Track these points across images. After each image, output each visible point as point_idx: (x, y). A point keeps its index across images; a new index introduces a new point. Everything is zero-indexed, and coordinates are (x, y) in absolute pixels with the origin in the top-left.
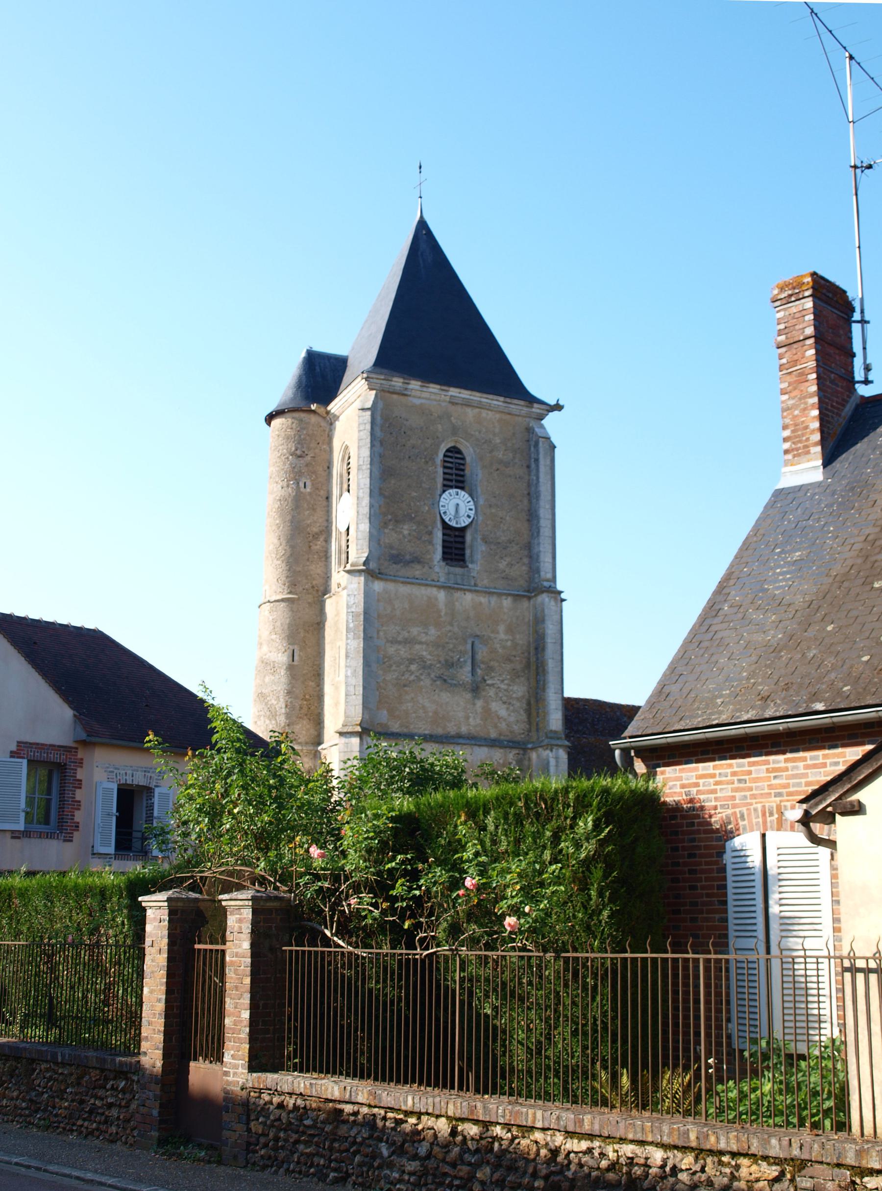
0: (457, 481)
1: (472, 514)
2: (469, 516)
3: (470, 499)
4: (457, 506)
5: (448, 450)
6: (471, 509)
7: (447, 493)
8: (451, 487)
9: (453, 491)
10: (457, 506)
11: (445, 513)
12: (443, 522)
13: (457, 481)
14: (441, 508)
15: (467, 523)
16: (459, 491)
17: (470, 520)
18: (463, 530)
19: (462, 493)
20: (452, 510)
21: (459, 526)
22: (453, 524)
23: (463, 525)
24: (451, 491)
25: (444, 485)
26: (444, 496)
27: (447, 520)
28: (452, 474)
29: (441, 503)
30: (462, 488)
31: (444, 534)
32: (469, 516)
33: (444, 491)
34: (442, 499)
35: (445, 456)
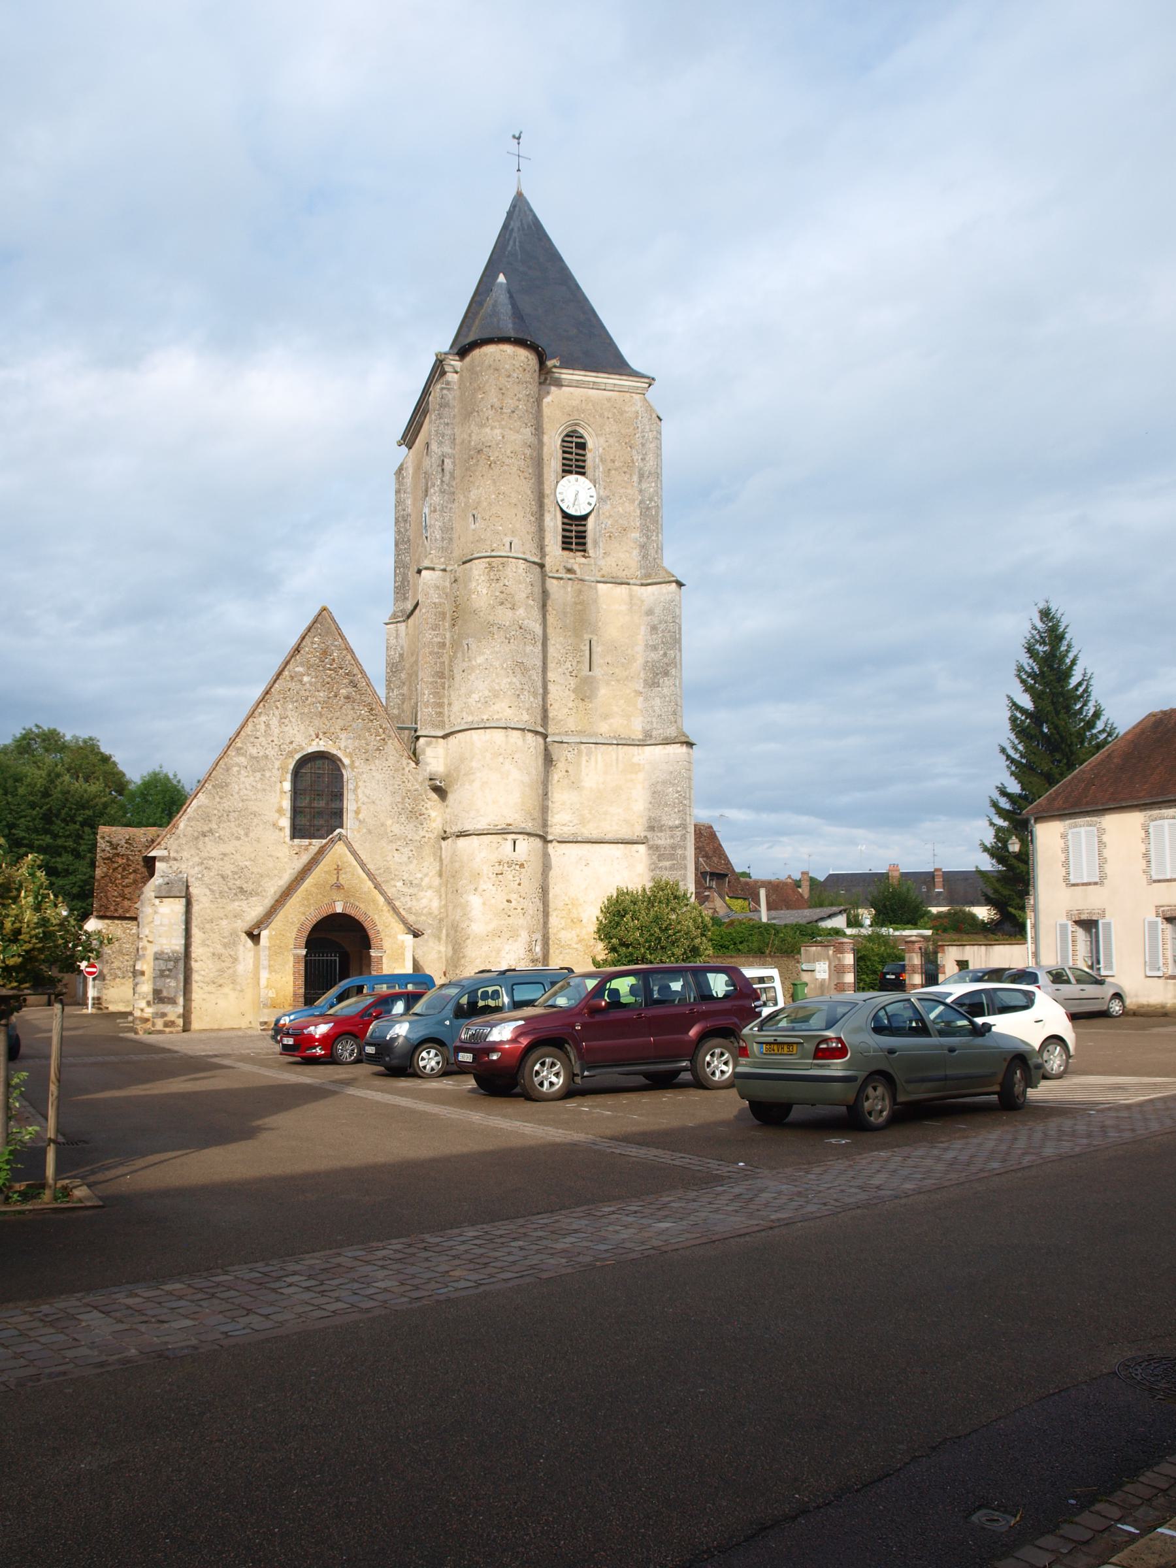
0: (577, 466)
1: (593, 501)
2: (590, 504)
4: (575, 494)
5: (567, 436)
8: (570, 472)
9: (572, 477)
10: (575, 494)
12: (562, 510)
13: (577, 466)
17: (590, 508)
18: (585, 518)
21: (578, 514)
22: (571, 511)
23: (584, 513)
25: (564, 471)
27: (565, 509)
30: (583, 474)
32: (590, 504)
35: (563, 441)
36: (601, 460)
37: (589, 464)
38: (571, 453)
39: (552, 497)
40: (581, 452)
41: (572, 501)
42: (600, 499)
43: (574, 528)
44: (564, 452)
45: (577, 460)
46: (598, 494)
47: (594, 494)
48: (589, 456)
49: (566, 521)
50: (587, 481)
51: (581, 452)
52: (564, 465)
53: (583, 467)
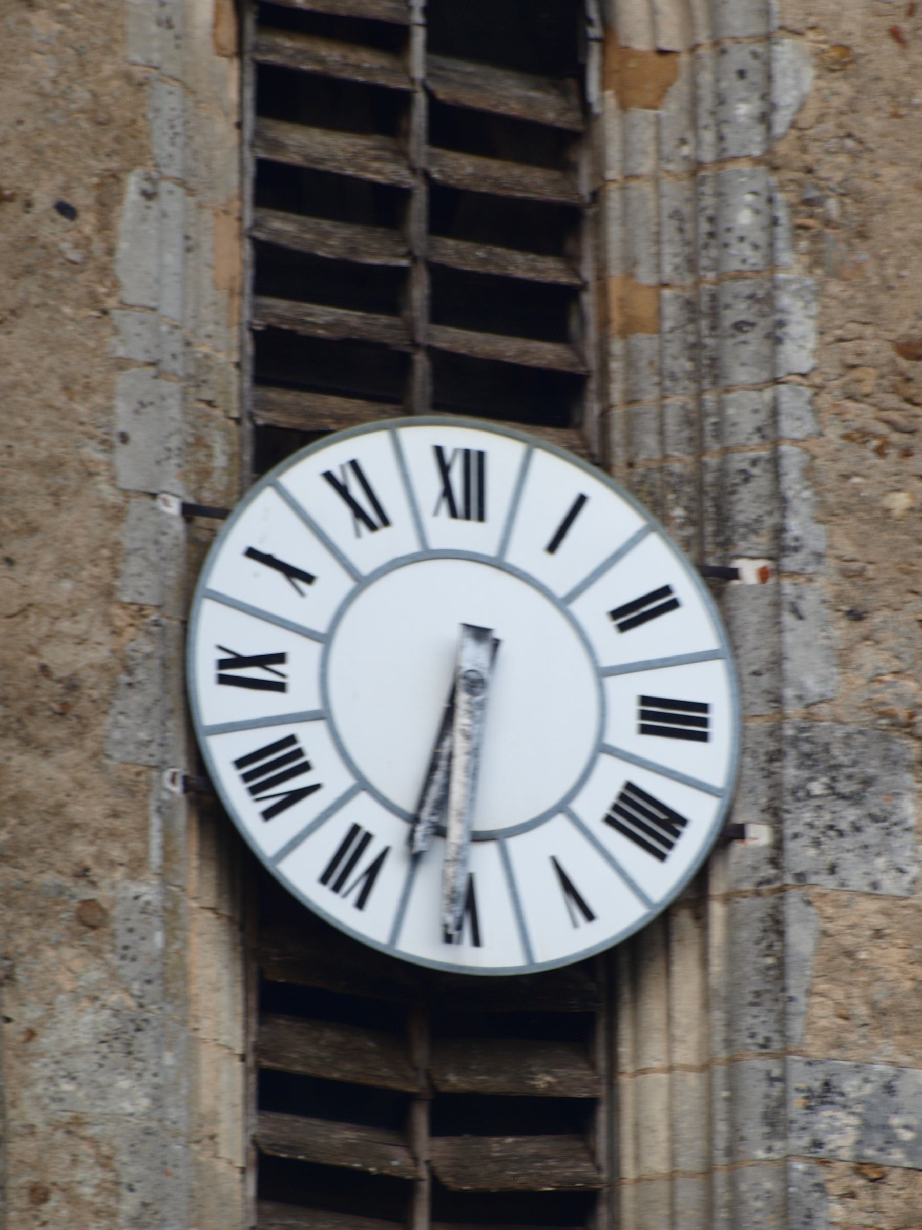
0: (461, 299)
1: (696, 777)
2: (645, 820)
3: (660, 563)
6: (673, 719)
7: (304, 475)
8: (379, 385)
9: (400, 454)
11: (277, 767)
13: (461, 299)
14: (215, 703)
15: (619, 915)
16: (502, 450)
17: (664, 878)
18: (581, 1004)
19: (532, 475)
20: (375, 732)
21: (497, 952)
22: (398, 920)
23: (561, 941)
24: (370, 448)
25: (277, 358)
26: (262, 520)
27: (302, 874)
28: (382, 206)
29: (216, 631)
30: (547, 404)
31: (273, 1090)
32: (645, 820)
33: (272, 449)
34: (228, 569)
36: (807, 217)
37: (637, 244)
38: (380, 111)
39: (131, 728)
40: (509, 94)
41: (402, 782)
42: (784, 753)
43: (425, 1154)
44: (278, 95)
45: (453, 210)
46: (761, 678)
47: (709, 685)
48: (636, 150)
49: (310, 1052)
50: (612, 515)
51: (509, 94)
52: (274, 269)
53: (550, 310)
